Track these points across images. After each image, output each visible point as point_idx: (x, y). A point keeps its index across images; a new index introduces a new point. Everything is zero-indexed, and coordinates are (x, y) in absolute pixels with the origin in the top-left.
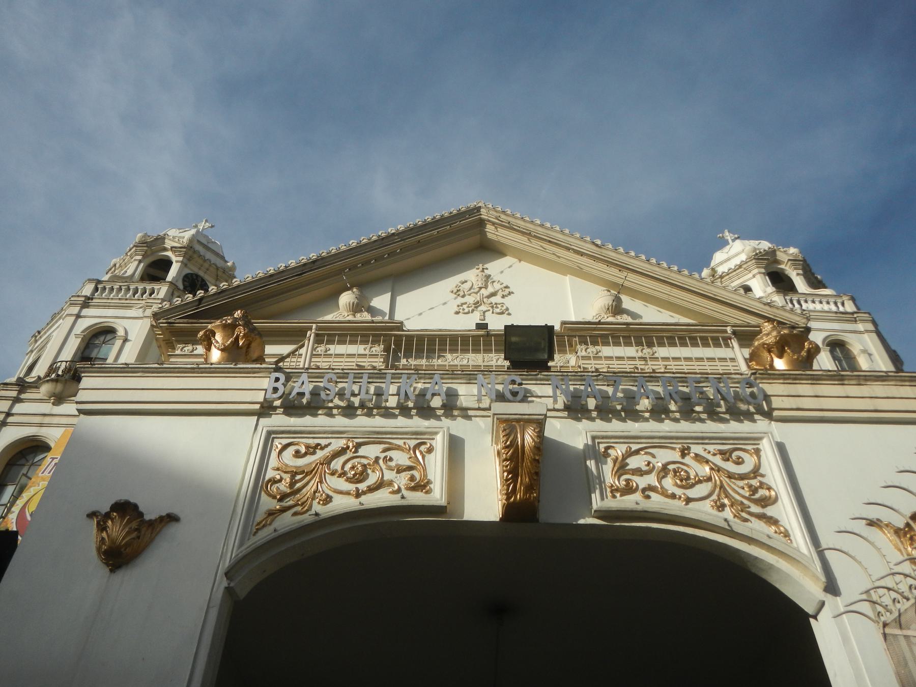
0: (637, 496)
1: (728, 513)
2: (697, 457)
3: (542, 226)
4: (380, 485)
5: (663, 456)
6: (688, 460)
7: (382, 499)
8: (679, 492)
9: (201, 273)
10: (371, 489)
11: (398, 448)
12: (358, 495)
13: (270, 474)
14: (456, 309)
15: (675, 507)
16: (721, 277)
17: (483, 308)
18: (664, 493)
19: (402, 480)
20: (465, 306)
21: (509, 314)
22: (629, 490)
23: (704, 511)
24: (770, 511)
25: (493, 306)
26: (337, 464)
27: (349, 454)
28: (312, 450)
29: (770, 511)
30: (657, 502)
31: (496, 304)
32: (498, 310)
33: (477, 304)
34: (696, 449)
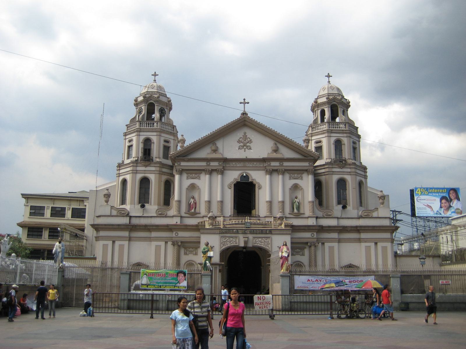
4: (232, 243)
6: (262, 240)
7: (233, 244)
8: (260, 244)
9: (163, 106)
12: (230, 244)
13: (222, 242)
15: (260, 245)
16: (318, 105)
17: (245, 147)
20: (241, 147)
22: (256, 243)
23: (262, 246)
25: (247, 147)
30: (258, 245)
32: (248, 148)
33: (244, 146)
34: (263, 238)
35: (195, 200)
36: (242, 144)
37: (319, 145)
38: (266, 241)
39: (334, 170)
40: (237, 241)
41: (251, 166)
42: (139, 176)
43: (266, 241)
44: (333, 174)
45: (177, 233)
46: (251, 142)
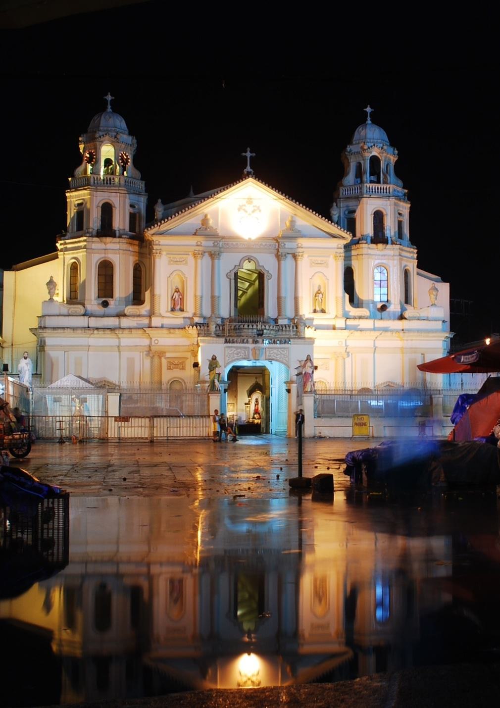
22: (270, 356)
26: (235, 352)
34: (279, 350)
38: (283, 353)
39: (370, 251)
40: (247, 352)
42: (97, 258)
43: (283, 353)
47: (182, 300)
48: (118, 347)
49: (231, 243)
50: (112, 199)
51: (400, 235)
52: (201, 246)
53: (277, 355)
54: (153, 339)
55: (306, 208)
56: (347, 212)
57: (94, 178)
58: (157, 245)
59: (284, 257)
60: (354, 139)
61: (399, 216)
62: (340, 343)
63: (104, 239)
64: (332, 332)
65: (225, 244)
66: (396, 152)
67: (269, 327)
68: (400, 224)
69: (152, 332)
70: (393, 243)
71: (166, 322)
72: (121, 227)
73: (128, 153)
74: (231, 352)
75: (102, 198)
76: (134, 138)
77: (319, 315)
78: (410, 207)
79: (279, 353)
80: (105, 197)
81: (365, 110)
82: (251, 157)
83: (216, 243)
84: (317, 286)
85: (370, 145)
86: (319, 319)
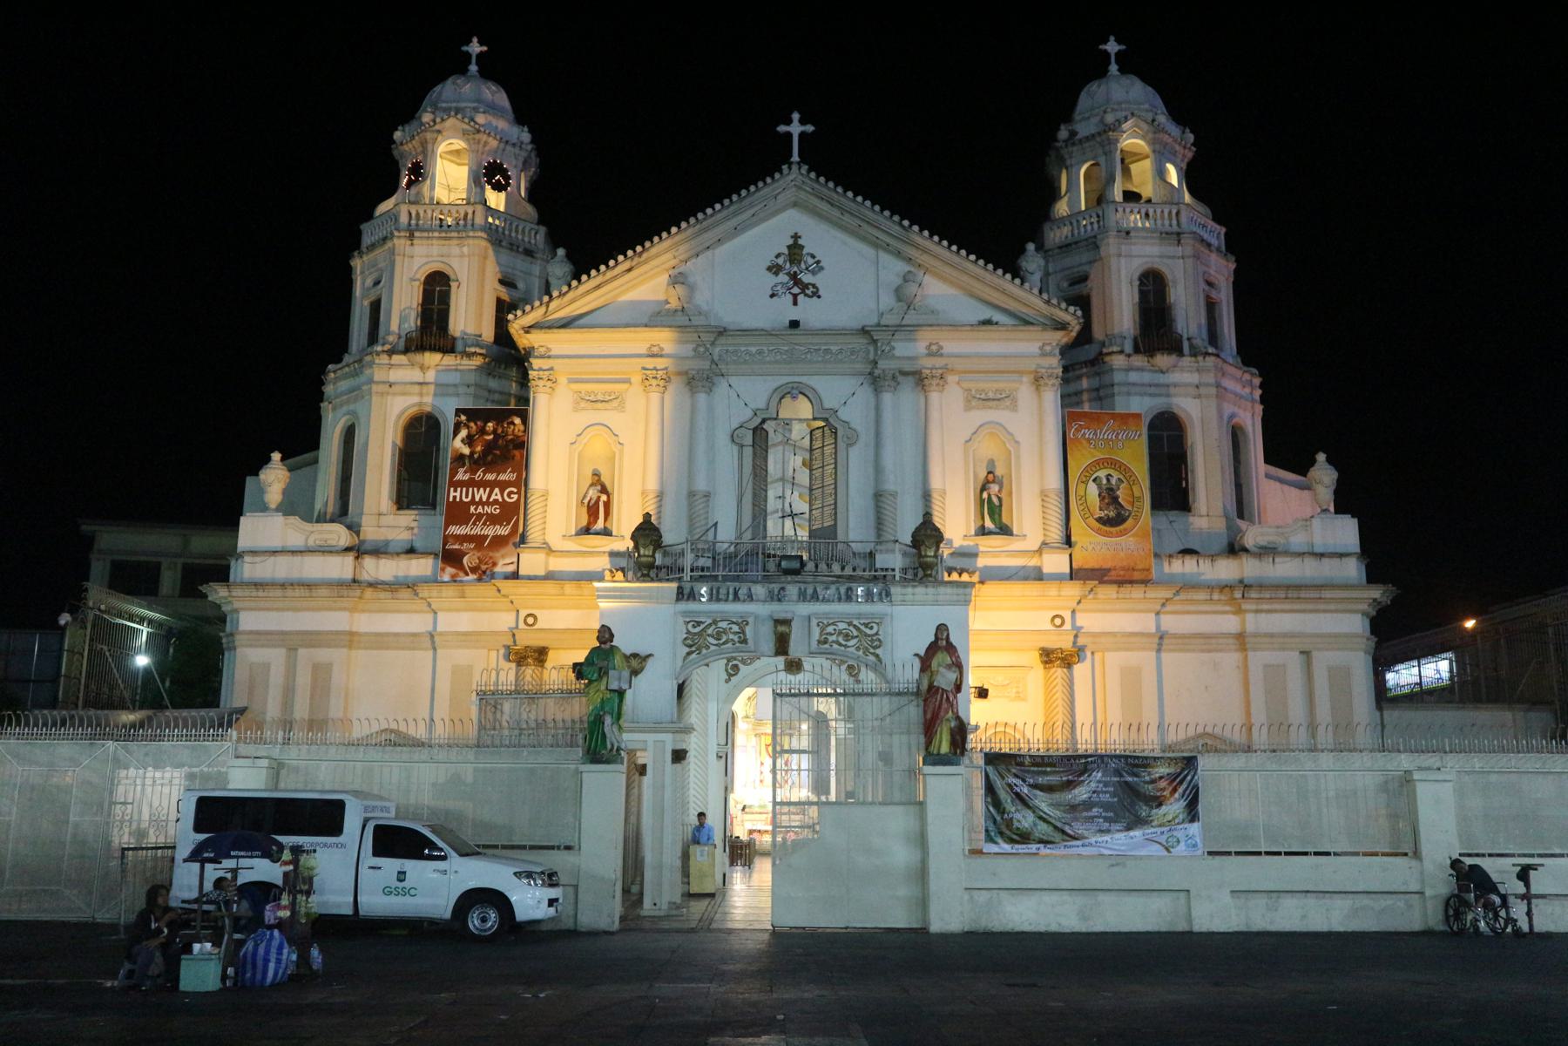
0: (827, 646)
1: (861, 653)
2: (855, 626)
3: (854, 201)
5: (842, 626)
8: (844, 643)
10: (724, 643)
11: (733, 623)
14: (771, 293)
17: (796, 290)
18: (840, 645)
19: (736, 638)
20: (779, 288)
21: (819, 297)
22: (825, 642)
24: (878, 651)
25: (804, 287)
27: (714, 627)
28: (699, 623)
29: (878, 651)
31: (810, 284)
35: (604, 490)
36: (783, 278)
37: (1078, 289)
38: (869, 632)
39: (1134, 377)
41: (820, 359)
43: (869, 632)
44: (1129, 394)
45: (535, 618)
46: (819, 267)
47: (607, 505)
48: (432, 636)
49: (743, 349)
50: (455, 263)
51: (1213, 337)
52: (661, 356)
53: (847, 637)
54: (523, 614)
55: (950, 245)
56: (1065, 285)
57: (410, 214)
58: (542, 357)
59: (893, 384)
60: (1077, 112)
61: (1207, 288)
62: (1058, 622)
63: (418, 357)
64: (1031, 589)
65: (727, 351)
66: (1191, 137)
67: (843, 568)
68: (1211, 306)
69: (523, 590)
70: (1194, 354)
71: (558, 564)
72: (471, 330)
73: (509, 164)
74: (697, 630)
75: (425, 260)
76: (526, 129)
77: (996, 542)
78: (1236, 271)
79: (855, 633)
80: (432, 256)
81: (1102, 47)
82: (802, 135)
83: (702, 349)
84: (985, 464)
85: (1121, 115)
86: (994, 553)
